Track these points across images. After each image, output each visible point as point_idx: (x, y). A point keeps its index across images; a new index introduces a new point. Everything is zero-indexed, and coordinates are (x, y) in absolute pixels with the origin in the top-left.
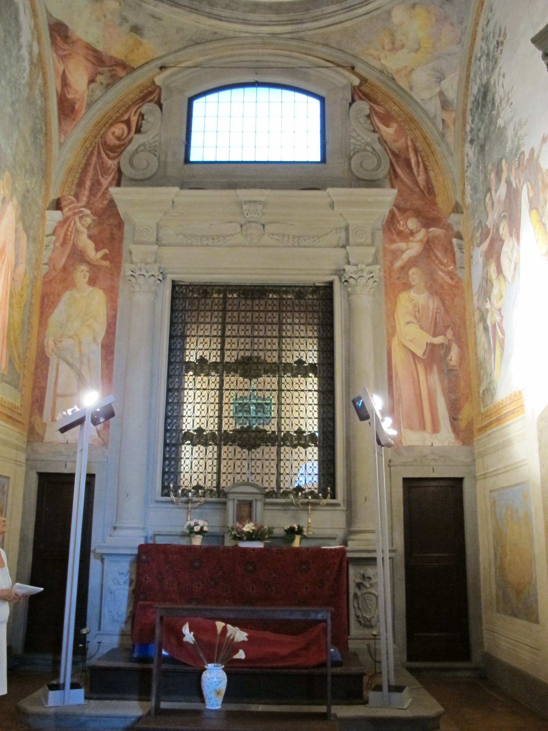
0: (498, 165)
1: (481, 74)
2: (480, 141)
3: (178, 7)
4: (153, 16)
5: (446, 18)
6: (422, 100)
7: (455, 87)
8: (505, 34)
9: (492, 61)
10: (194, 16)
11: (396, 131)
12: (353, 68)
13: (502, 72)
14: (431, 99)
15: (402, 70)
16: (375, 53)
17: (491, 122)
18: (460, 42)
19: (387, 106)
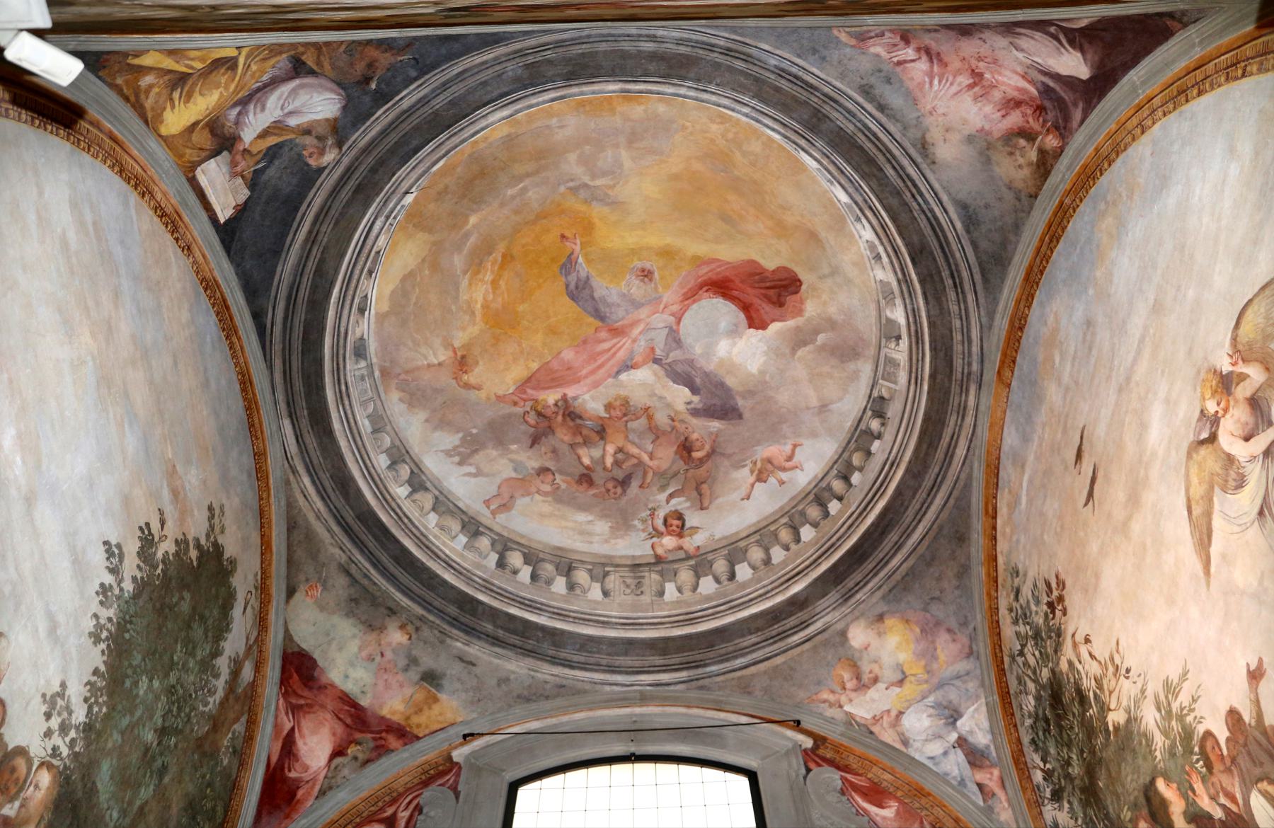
0: (1148, 799)
1: (1034, 672)
2: (1077, 782)
3: (504, 648)
4: (461, 659)
5: (938, 624)
6: (932, 758)
7: (986, 724)
8: (1061, 584)
9: (1050, 637)
10: (530, 662)
11: (898, 813)
12: (798, 722)
13: (1080, 638)
14: (945, 753)
15: (882, 717)
16: (831, 698)
17: (1090, 731)
18: (970, 654)
19: (870, 775)
